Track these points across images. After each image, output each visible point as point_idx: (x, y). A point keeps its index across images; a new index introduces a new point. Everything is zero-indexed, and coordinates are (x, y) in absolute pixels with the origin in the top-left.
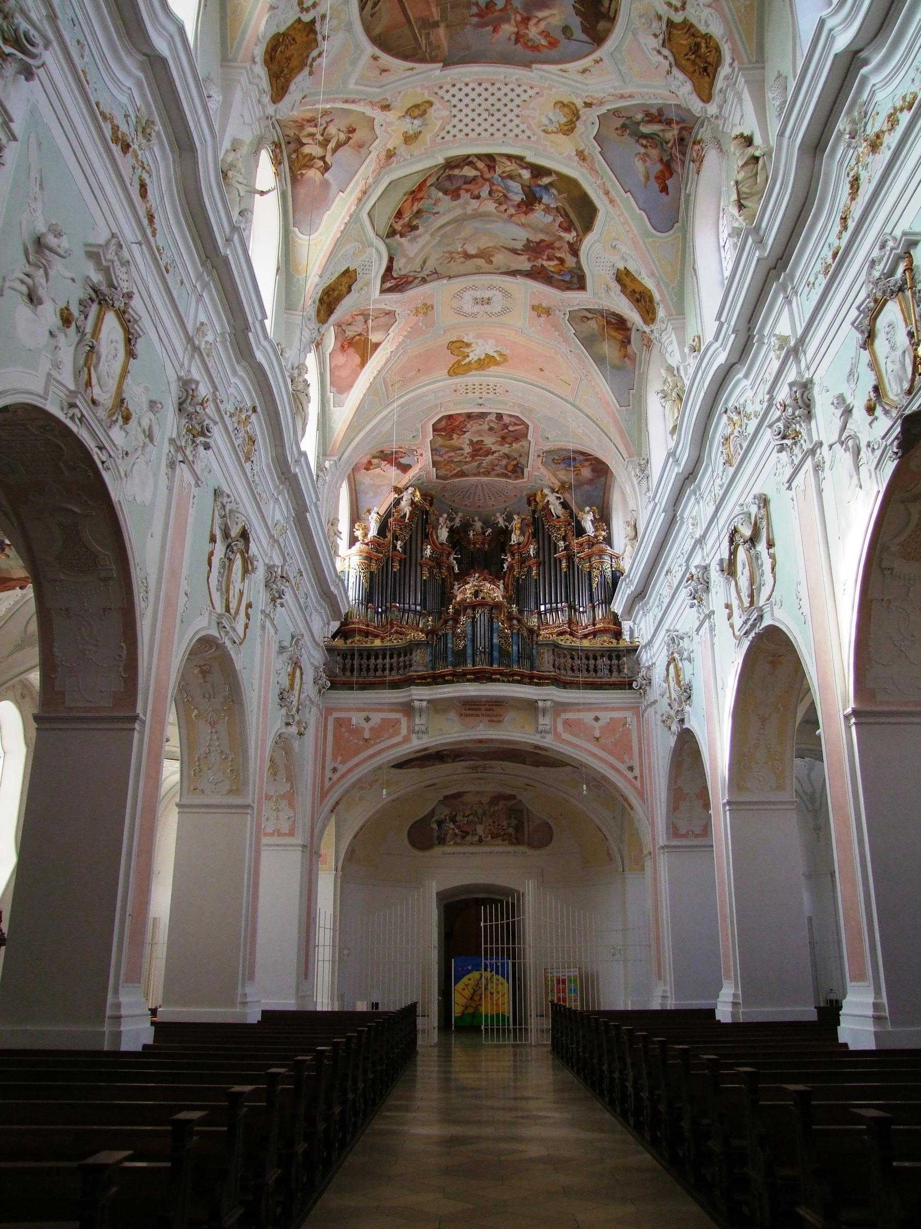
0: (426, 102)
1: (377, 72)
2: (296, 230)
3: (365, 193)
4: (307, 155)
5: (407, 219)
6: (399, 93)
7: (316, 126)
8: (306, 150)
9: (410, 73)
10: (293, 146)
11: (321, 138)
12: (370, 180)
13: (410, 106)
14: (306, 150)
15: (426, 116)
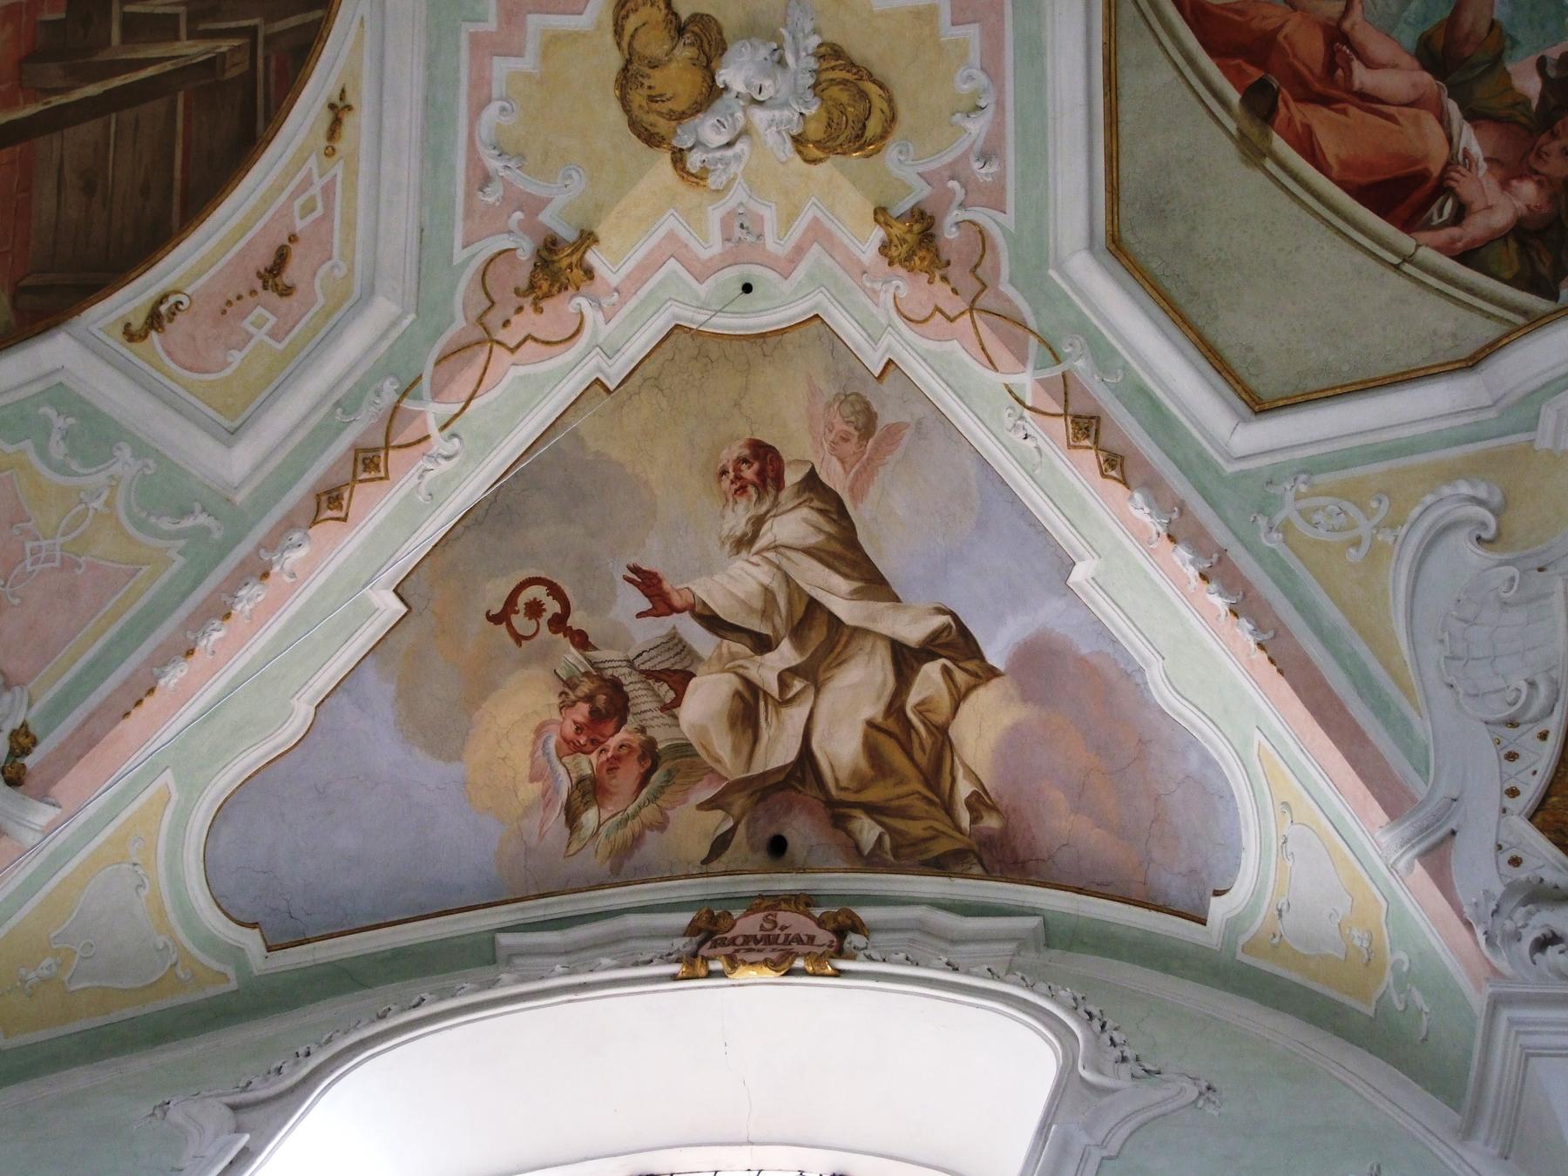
0: (618, 31)
1: (261, 317)
2: (1218, 909)
3: (1086, 426)
4: (871, 750)
5: (1470, 140)
6: (487, 179)
7: (680, 680)
8: (841, 749)
9: (359, 124)
10: (801, 830)
11: (786, 655)
12: (1025, 381)
13: (614, 114)
14: (841, 749)
15: (729, 16)
